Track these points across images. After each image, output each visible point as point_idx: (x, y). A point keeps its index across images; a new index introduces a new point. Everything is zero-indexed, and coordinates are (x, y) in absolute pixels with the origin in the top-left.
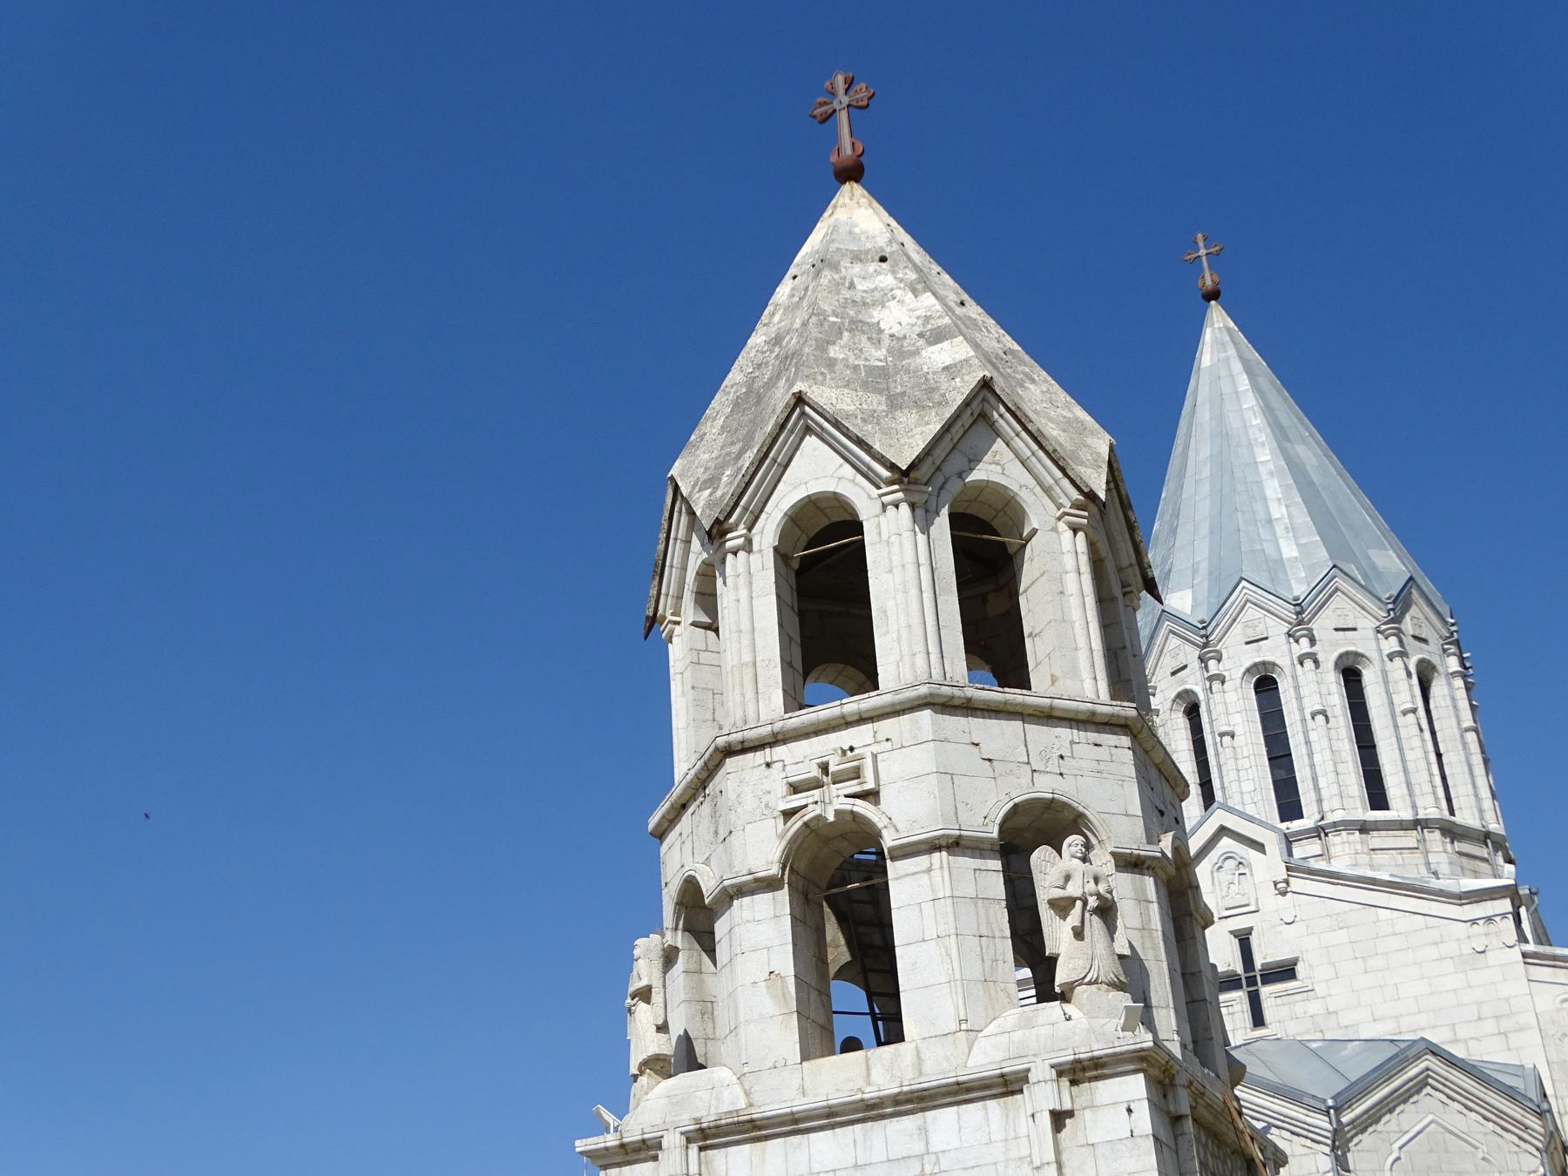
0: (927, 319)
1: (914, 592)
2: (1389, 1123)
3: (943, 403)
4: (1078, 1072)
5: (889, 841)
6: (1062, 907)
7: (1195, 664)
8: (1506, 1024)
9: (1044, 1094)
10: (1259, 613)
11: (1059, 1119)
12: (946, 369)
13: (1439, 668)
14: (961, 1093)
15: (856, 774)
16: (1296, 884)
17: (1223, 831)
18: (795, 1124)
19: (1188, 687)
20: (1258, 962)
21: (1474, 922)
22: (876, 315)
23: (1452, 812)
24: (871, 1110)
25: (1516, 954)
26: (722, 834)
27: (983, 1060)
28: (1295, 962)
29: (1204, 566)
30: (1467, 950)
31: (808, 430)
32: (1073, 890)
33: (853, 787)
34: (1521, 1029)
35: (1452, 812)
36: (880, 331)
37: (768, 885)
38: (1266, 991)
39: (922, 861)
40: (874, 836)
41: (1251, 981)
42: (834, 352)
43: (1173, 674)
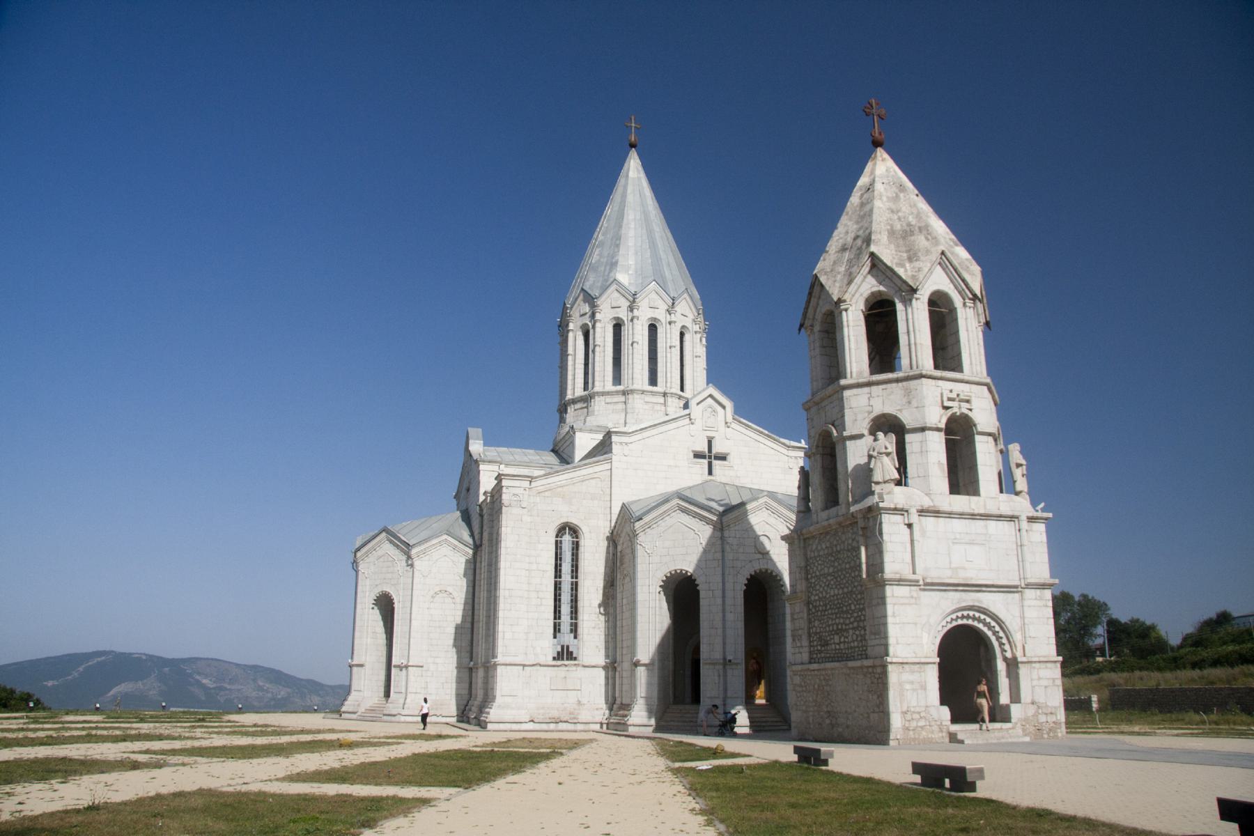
4: (1031, 519)
5: (980, 428)
14: (1000, 517)
16: (733, 425)
17: (710, 396)
18: (950, 515)
24: (973, 516)
27: (1005, 510)
37: (938, 430)
38: (715, 463)
41: (710, 457)
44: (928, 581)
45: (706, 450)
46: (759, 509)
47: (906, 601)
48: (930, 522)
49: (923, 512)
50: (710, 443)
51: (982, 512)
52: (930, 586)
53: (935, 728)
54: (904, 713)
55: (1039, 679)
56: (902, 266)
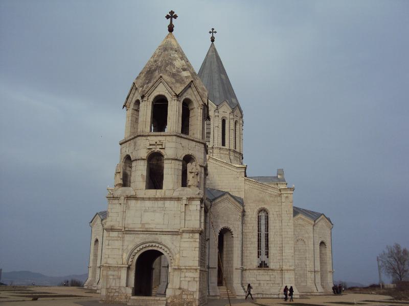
0: (183, 65)
1: (175, 116)
3: (185, 83)
4: (190, 199)
5: (165, 157)
6: (191, 173)
9: (185, 202)
14: (171, 199)
15: (162, 145)
18: (143, 199)
22: (174, 62)
24: (156, 199)
25: (243, 179)
27: (176, 194)
32: (193, 171)
33: (161, 147)
34: (242, 191)
40: (162, 156)
42: (168, 68)
44: (127, 229)
47: (116, 238)
48: (132, 203)
49: (128, 198)
51: (160, 196)
52: (128, 231)
53: (124, 297)
54: (107, 289)
55: (185, 277)
56: (142, 86)
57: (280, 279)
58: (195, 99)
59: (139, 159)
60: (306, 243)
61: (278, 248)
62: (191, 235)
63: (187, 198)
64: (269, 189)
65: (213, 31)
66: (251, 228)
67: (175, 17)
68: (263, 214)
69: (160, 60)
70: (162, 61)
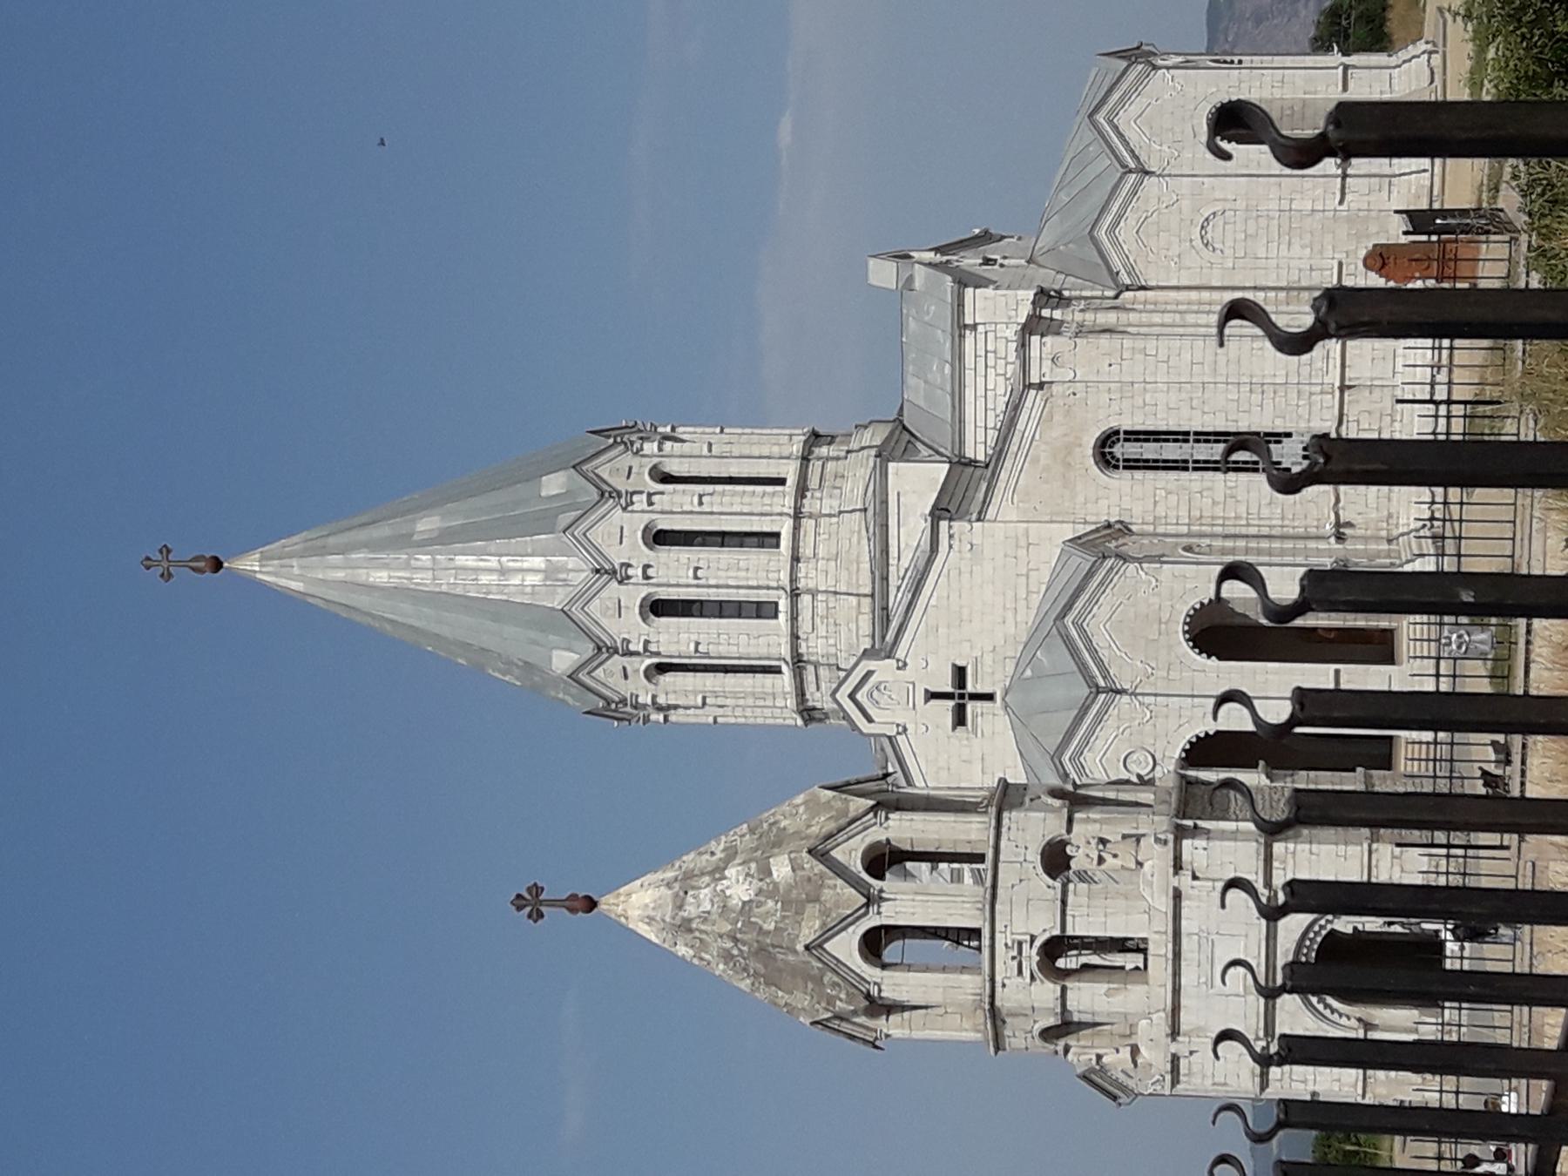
0: (747, 875)
2: (1104, 654)
3: (822, 876)
4: (1178, 866)
5: (1057, 932)
7: (626, 660)
8: (1023, 543)
9: (1185, 880)
10: (596, 601)
11: (1195, 877)
12: (794, 870)
13: (656, 460)
16: (900, 654)
17: (852, 696)
19: (643, 668)
20: (950, 689)
21: (951, 547)
22: (735, 902)
23: (781, 481)
25: (977, 525)
26: (1029, 1012)
27: (1164, 904)
28: (954, 665)
29: (533, 634)
30: (969, 555)
31: (820, 946)
35: (781, 481)
36: (750, 901)
37: (1064, 990)
38: (970, 688)
39: (1069, 919)
41: (962, 696)
42: (770, 926)
43: (626, 677)
44: (1261, 1034)
45: (951, 703)
46: (1081, 769)
50: (933, 696)
56: (831, 1001)
57: (1377, 393)
58: (859, 837)
59: (1064, 1005)
60: (1219, 207)
61: (1256, 398)
62: (1275, 864)
63: (1176, 873)
64: (1020, 426)
65: (163, 563)
66: (1173, 499)
67: (536, 890)
68: (1121, 450)
69: (729, 945)
70: (735, 940)
